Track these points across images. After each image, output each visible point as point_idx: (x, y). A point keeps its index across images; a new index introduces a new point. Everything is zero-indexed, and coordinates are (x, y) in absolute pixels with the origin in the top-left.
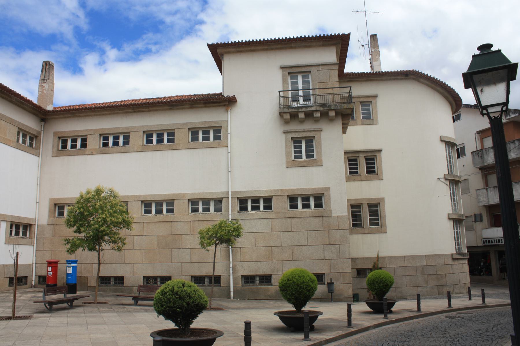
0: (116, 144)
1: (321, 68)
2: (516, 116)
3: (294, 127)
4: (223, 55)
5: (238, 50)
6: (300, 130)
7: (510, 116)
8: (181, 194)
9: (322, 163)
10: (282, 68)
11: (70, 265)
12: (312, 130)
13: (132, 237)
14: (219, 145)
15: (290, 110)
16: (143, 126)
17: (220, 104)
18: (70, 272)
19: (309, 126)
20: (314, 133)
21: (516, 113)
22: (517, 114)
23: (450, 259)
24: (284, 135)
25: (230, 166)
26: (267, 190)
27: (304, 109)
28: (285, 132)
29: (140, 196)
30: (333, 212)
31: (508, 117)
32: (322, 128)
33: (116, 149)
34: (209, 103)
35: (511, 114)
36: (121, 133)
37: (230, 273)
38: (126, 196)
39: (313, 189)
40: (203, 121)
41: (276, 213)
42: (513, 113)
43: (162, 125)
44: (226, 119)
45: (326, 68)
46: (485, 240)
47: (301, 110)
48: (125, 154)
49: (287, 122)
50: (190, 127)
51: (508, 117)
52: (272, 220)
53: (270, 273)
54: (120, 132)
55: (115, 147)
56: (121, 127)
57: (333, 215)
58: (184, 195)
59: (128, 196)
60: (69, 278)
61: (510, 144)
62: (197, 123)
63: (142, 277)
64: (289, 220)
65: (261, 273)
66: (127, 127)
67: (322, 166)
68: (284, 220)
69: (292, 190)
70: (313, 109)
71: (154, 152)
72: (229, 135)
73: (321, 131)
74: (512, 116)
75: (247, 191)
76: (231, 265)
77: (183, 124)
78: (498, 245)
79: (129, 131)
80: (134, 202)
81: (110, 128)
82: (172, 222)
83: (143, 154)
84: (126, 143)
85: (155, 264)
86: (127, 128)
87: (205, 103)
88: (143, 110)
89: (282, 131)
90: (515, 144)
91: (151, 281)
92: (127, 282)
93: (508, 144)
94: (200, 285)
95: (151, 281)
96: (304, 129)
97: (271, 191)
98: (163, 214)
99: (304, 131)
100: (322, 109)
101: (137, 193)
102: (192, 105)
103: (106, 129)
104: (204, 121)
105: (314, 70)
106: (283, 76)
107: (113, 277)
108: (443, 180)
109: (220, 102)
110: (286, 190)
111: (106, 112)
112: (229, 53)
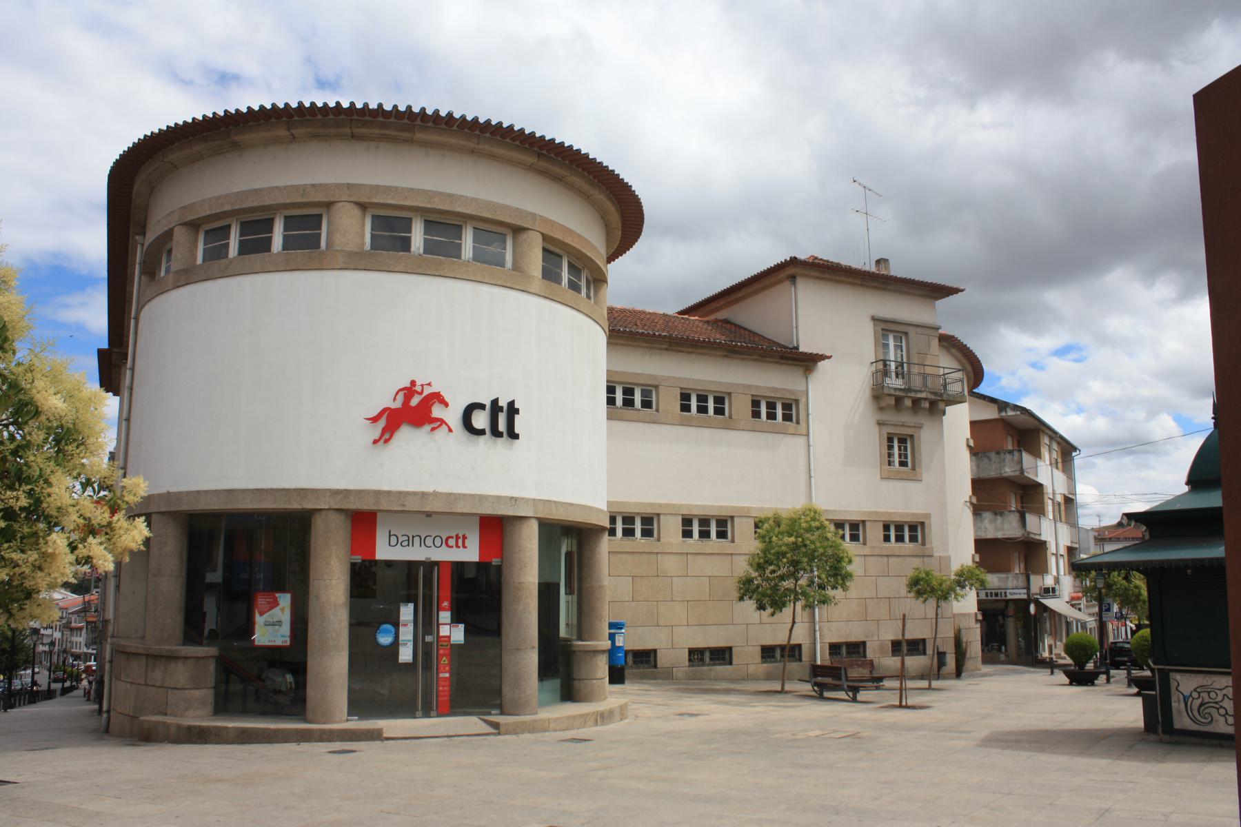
0: (628, 403)
1: (919, 330)
2: (1017, 415)
3: (891, 417)
4: (795, 277)
5: (822, 276)
6: (899, 424)
7: (1006, 412)
8: (744, 507)
9: (922, 477)
10: (875, 319)
11: (619, 631)
12: (912, 425)
13: (670, 579)
14: (796, 431)
15: (897, 393)
16: (679, 379)
17: (802, 363)
18: (621, 645)
19: (907, 418)
20: (913, 429)
21: (1017, 410)
22: (1018, 413)
23: (974, 620)
24: (877, 428)
25: (812, 468)
26: (858, 512)
27: (913, 394)
28: (880, 424)
29: (681, 506)
30: (935, 549)
31: (1004, 414)
32: (922, 424)
33: (628, 412)
34: (788, 359)
35: (1008, 410)
36: (637, 385)
37: (815, 639)
38: (656, 504)
39: (913, 514)
40: (772, 386)
41: (870, 547)
42: (1011, 409)
43: (711, 382)
44: (803, 388)
45: (925, 331)
46: (989, 591)
47: (909, 395)
48: (652, 425)
49: (881, 409)
50: (754, 394)
51: (1004, 414)
52: (866, 558)
53: (863, 640)
54: (642, 382)
55: (628, 409)
56: (643, 374)
57: (935, 554)
58: (749, 509)
59: (660, 505)
60: (620, 655)
61: (1005, 454)
62: (762, 387)
63: (687, 650)
64: (885, 559)
65: (852, 639)
66: (654, 376)
67: (921, 481)
68: (879, 559)
69: (888, 513)
70: (923, 395)
71: (700, 429)
72: (810, 416)
73: (920, 427)
74: (1010, 413)
75: (834, 511)
76: (817, 628)
77: (745, 386)
78: (996, 601)
79: (657, 384)
80: (669, 517)
81: (623, 372)
82: (732, 554)
83: (681, 428)
84: (647, 404)
85: (708, 627)
86: (654, 377)
87: (782, 358)
88: (680, 349)
89: (876, 420)
90: (1013, 455)
91: (696, 657)
92: (662, 660)
93: (1002, 454)
94: (769, 660)
95: (696, 657)
96: (903, 422)
97: (864, 513)
98: (712, 540)
99: (903, 426)
100: (933, 397)
101: (675, 501)
102: (764, 357)
103: (617, 372)
104: (774, 388)
105: (912, 331)
106: (875, 333)
107: (632, 650)
108: (968, 504)
109: (802, 361)
110: (882, 513)
111: (622, 342)
112: (806, 276)
